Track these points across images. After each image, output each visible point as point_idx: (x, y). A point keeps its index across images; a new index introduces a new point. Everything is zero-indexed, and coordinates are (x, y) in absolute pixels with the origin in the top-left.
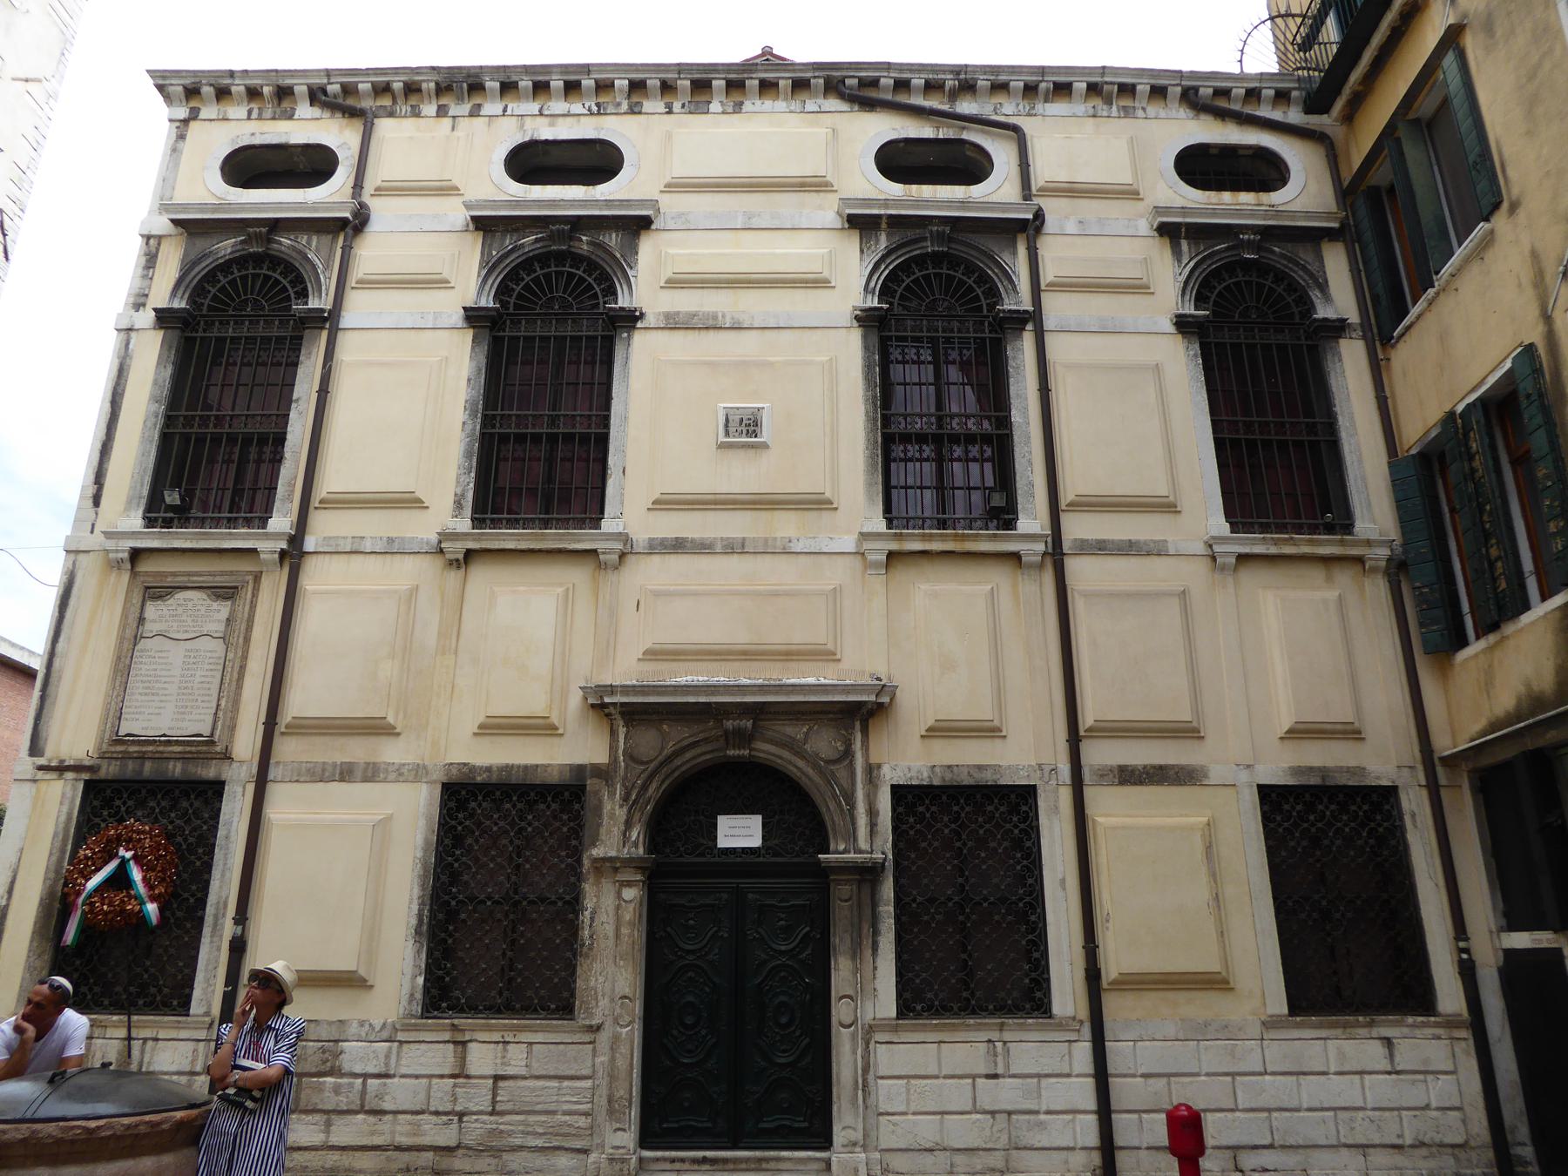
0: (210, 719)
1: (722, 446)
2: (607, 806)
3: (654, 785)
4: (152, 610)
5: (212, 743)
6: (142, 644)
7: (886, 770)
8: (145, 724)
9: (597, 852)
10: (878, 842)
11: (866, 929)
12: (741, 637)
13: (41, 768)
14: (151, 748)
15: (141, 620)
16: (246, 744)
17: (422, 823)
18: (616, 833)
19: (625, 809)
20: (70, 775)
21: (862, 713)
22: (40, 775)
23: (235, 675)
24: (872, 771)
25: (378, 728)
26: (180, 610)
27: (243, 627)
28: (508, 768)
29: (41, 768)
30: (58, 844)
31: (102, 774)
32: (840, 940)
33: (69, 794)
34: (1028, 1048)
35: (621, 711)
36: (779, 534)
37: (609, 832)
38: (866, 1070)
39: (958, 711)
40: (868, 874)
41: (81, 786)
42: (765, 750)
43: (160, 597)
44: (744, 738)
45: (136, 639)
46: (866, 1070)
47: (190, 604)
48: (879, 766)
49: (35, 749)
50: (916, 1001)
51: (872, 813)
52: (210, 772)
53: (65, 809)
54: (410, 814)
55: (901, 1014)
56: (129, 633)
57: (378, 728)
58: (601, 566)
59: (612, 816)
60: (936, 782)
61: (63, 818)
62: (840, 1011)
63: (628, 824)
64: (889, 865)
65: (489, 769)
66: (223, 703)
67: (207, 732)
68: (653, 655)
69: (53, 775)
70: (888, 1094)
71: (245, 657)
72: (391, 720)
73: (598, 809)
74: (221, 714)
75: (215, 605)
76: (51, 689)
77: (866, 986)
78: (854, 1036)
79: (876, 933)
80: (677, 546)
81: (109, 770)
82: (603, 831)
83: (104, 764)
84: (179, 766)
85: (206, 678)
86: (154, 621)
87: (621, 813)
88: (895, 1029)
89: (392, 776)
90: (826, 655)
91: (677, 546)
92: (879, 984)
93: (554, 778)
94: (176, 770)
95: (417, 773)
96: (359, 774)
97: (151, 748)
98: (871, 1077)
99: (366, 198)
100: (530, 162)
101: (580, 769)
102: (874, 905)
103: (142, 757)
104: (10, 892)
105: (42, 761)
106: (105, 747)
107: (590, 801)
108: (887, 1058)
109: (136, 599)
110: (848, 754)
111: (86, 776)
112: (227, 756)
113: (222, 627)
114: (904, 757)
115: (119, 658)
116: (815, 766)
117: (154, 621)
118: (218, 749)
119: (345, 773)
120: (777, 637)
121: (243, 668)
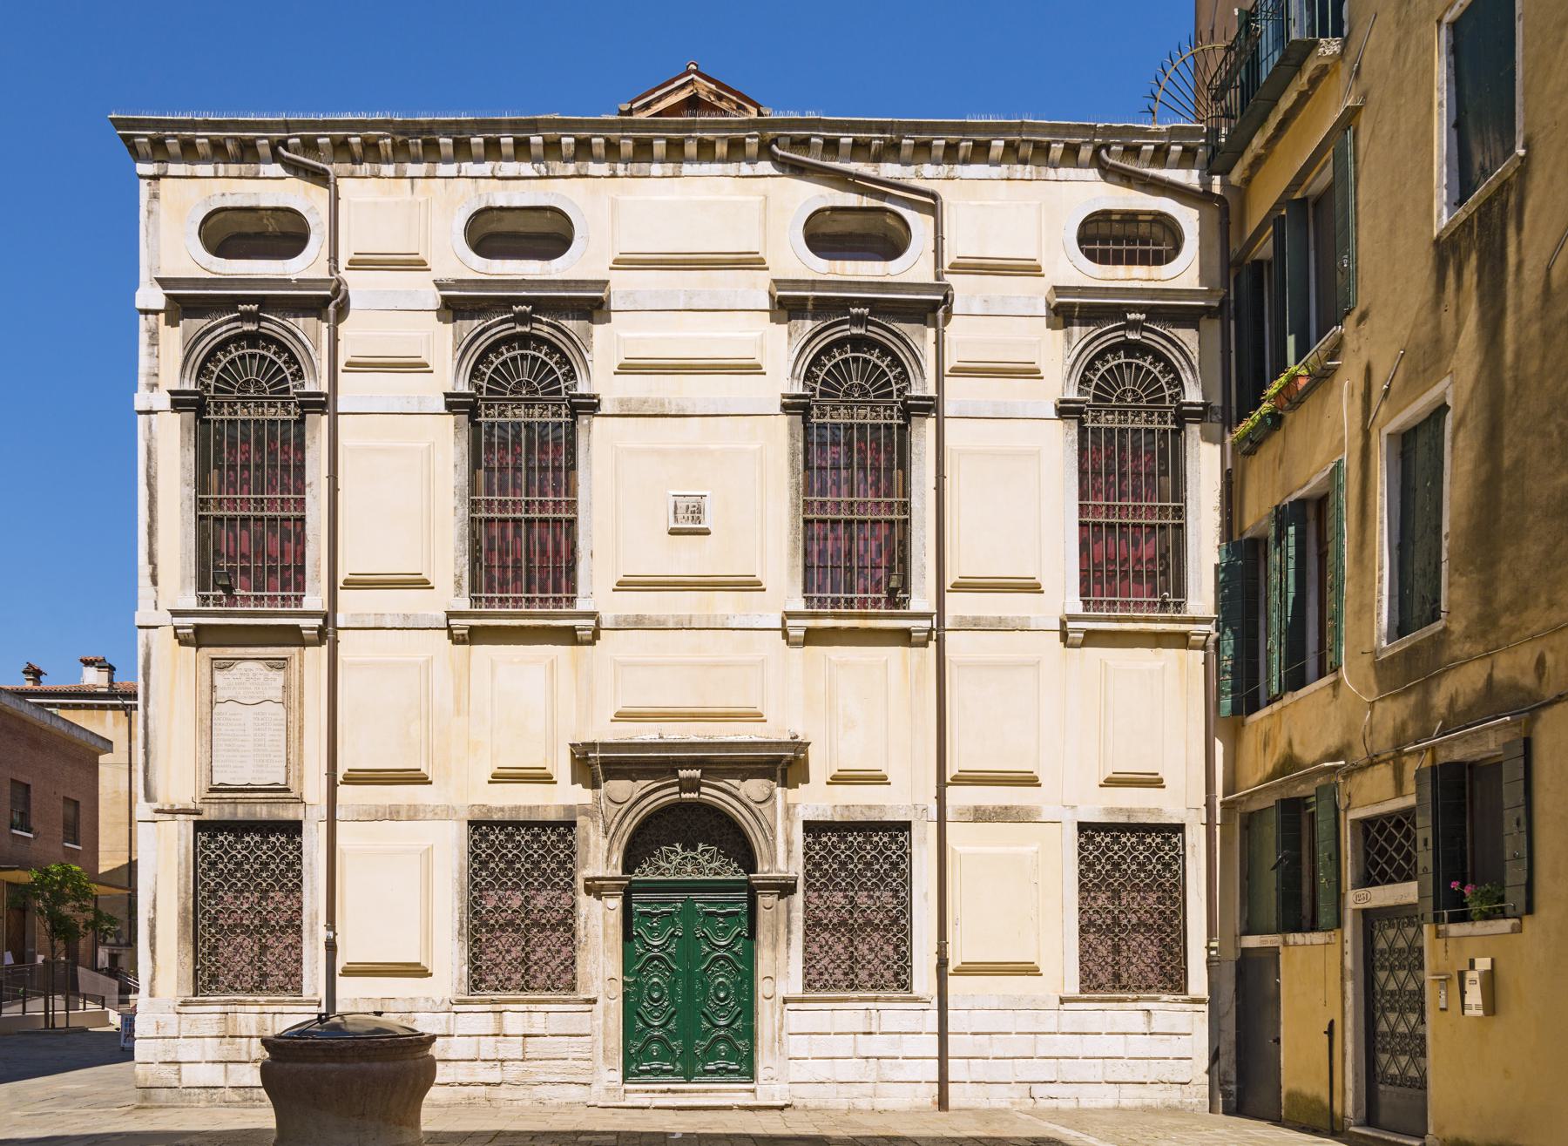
0: (283, 771)
1: (673, 532)
2: (593, 839)
3: (628, 821)
5: (288, 790)
7: (799, 809)
9: (589, 873)
10: (793, 863)
11: (782, 929)
12: (689, 702)
13: (157, 811)
16: (314, 789)
17: (456, 851)
18: (599, 856)
19: (607, 841)
20: (181, 817)
21: (785, 764)
22: (158, 817)
24: (788, 809)
25: (417, 778)
28: (517, 808)
29: (157, 811)
30: (183, 871)
31: (205, 817)
32: (763, 935)
33: (184, 832)
34: (894, 1015)
35: (595, 764)
36: (719, 613)
37: (595, 857)
38: (781, 1029)
39: (855, 761)
40: (785, 889)
41: (191, 825)
42: (708, 794)
44: (693, 785)
46: (781, 1029)
48: (795, 805)
49: (149, 797)
50: (816, 981)
51: (789, 842)
52: (288, 813)
53: (183, 843)
54: (448, 847)
55: (808, 985)
56: (206, 698)
57: (417, 778)
58: (575, 641)
59: (597, 846)
60: (837, 819)
61: (183, 851)
62: (763, 988)
63: (609, 850)
64: (800, 883)
65: (502, 810)
68: (621, 716)
69: (168, 817)
70: (796, 1046)
71: (301, 719)
72: (423, 770)
73: (586, 839)
76: (151, 747)
77: (781, 965)
78: (772, 1006)
79: (789, 932)
80: (637, 624)
81: (211, 813)
82: (591, 856)
83: (206, 807)
84: (264, 808)
85: (275, 737)
87: (604, 843)
88: (802, 1000)
89: (429, 816)
90: (758, 717)
91: (637, 624)
92: (791, 969)
93: (552, 816)
94: (263, 813)
95: (447, 813)
96: (403, 815)
98: (784, 1033)
99: (344, 274)
100: (490, 233)
101: (569, 809)
102: (789, 912)
103: (235, 802)
104: (154, 908)
105: (157, 806)
106: (204, 795)
107: (579, 831)
108: (800, 1019)
110: (771, 796)
111: (195, 817)
112: (300, 801)
114: (817, 799)
116: (746, 806)
119: (393, 814)
120: (717, 703)
121: (301, 728)
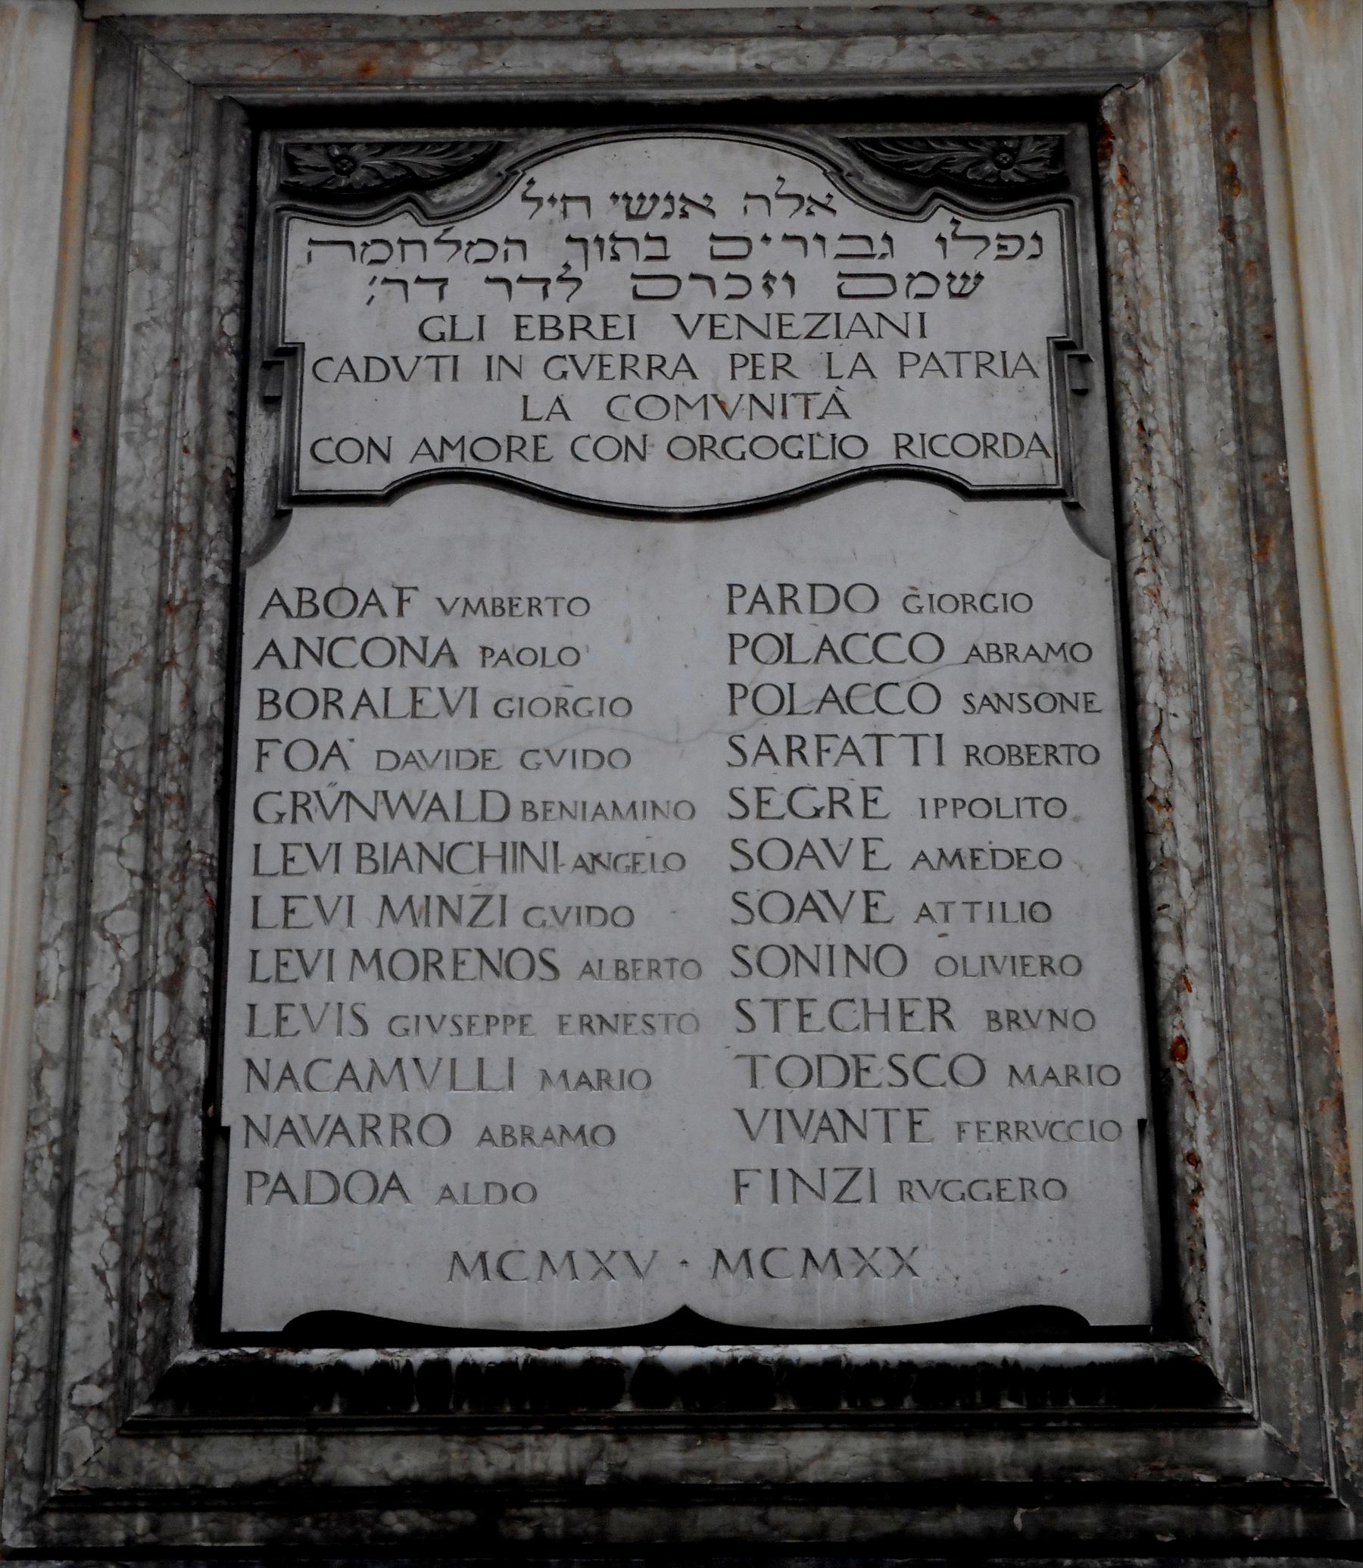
0: (1117, 1177)
4: (333, 286)
5: (1168, 1384)
6: (305, 554)
8: (483, 1228)
14: (554, 1455)
15: (263, 364)
23: (1245, 812)
26: (606, 285)
27: (1208, 414)
43: (402, 189)
45: (242, 511)
47: (688, 244)
66: (1195, 1023)
67: (1110, 1279)
74: (1199, 1129)
75: (920, 242)
86: (369, 370)
97: (554, 1455)
109: (169, 208)
113: (1026, 407)
115: (85, 683)
117: (369, 370)
118: (1247, 1451)
